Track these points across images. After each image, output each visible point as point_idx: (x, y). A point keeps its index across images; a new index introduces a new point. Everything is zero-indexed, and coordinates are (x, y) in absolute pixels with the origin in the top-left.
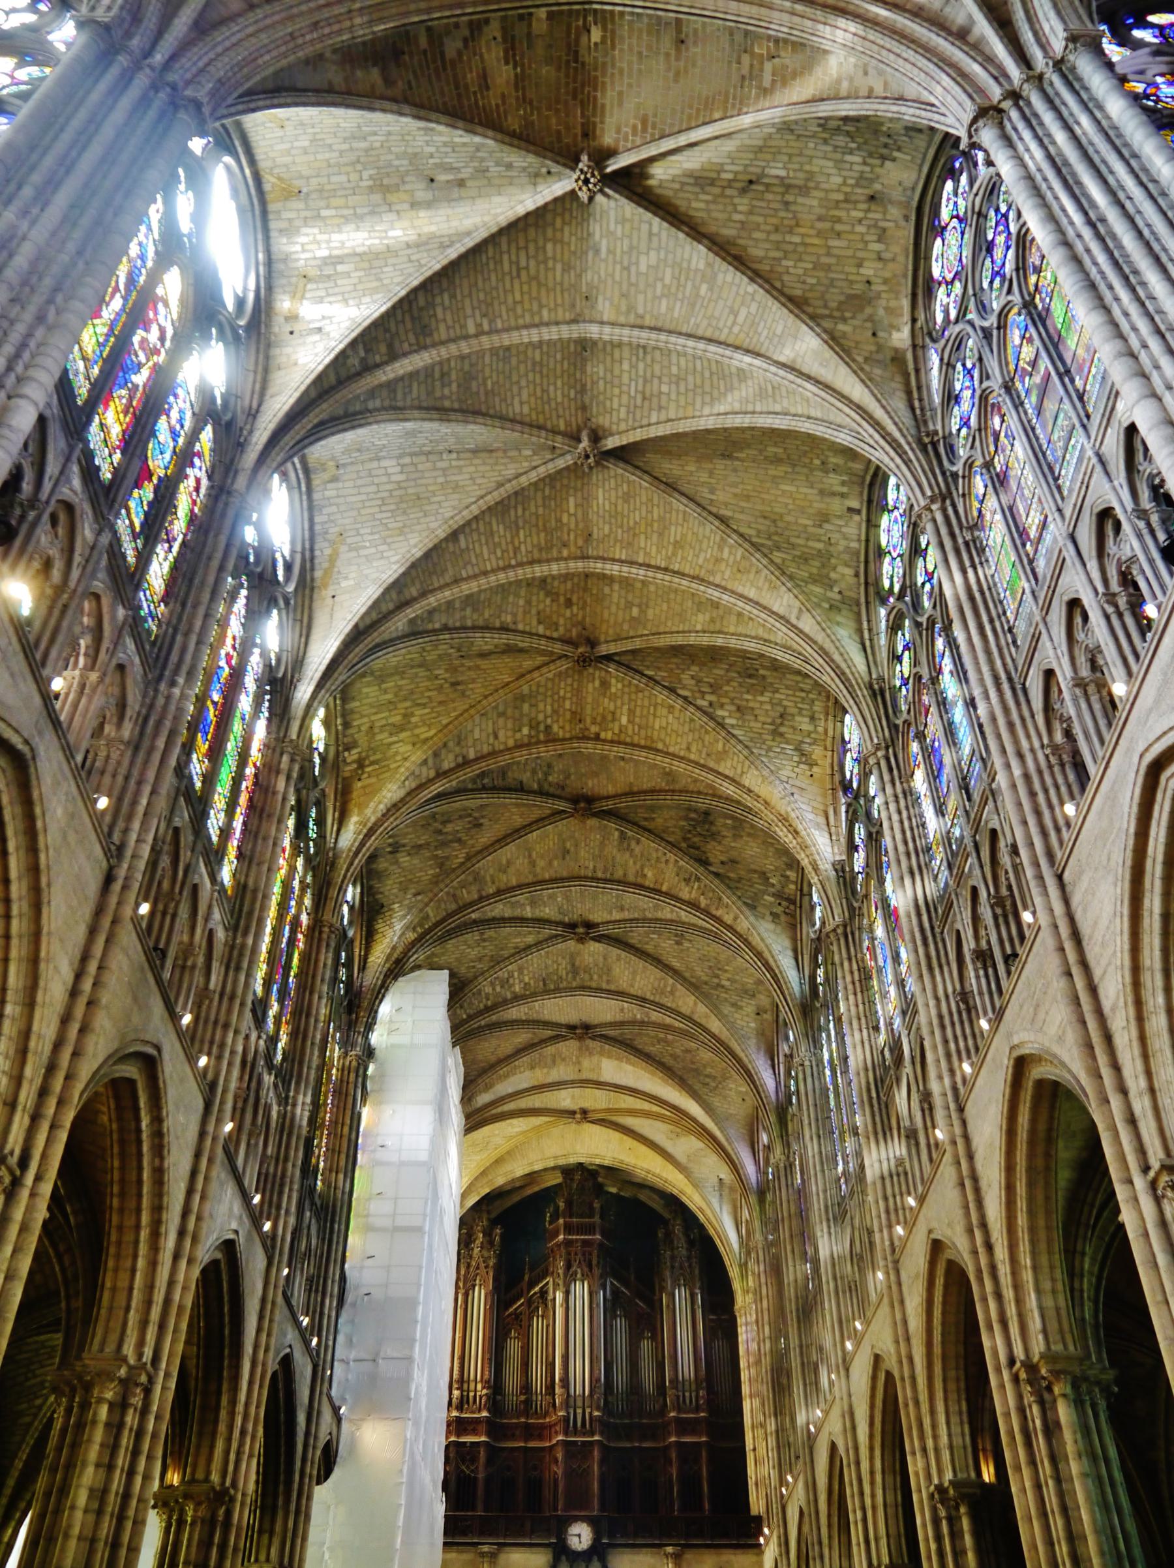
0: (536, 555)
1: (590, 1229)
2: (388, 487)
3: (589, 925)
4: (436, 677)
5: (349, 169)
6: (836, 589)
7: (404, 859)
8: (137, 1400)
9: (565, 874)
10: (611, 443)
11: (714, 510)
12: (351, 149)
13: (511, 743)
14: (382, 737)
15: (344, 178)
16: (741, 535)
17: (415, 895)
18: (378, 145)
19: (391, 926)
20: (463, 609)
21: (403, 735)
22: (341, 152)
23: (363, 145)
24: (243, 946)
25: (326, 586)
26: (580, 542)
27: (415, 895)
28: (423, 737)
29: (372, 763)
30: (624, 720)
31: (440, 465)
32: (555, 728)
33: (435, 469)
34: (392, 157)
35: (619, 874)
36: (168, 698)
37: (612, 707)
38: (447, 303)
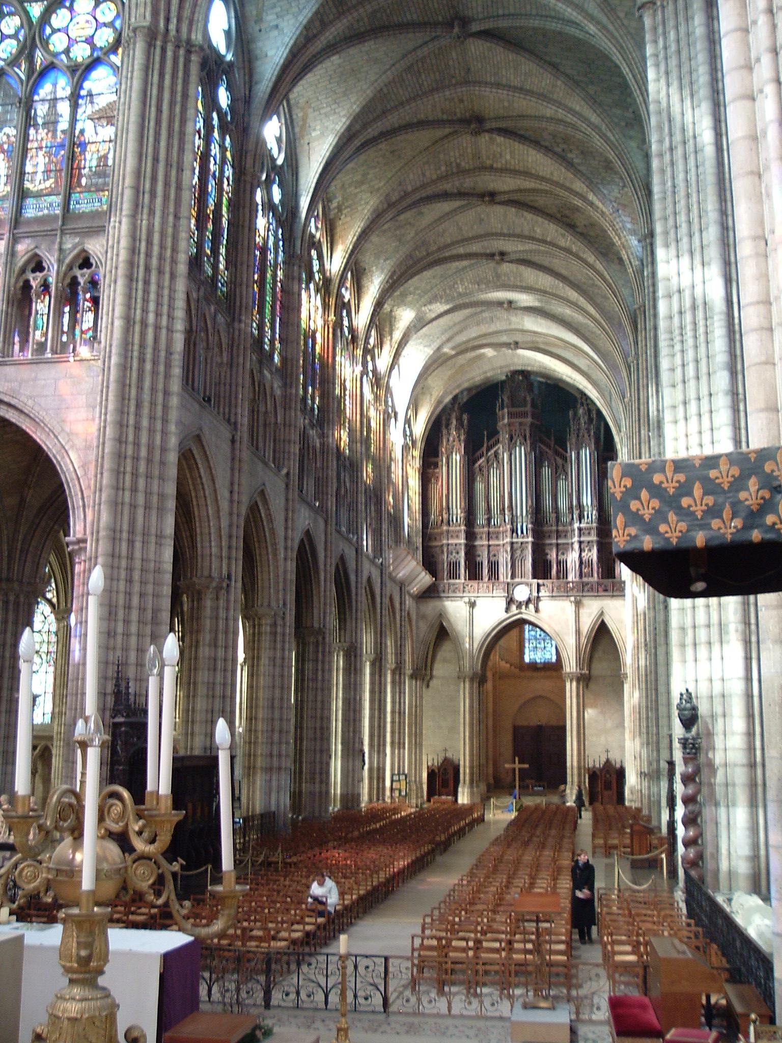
0: (434, 85)
1: (524, 415)
3: (502, 254)
6: (631, 110)
8: (279, 622)
9: (482, 233)
10: (475, 27)
11: (548, 59)
13: (435, 177)
16: (567, 75)
17: (385, 261)
19: (372, 282)
21: (364, 187)
24: (291, 394)
25: (303, 137)
26: (463, 74)
28: (376, 187)
29: (346, 208)
30: (508, 157)
32: (463, 164)
35: (518, 231)
36: (239, 330)
37: (499, 150)
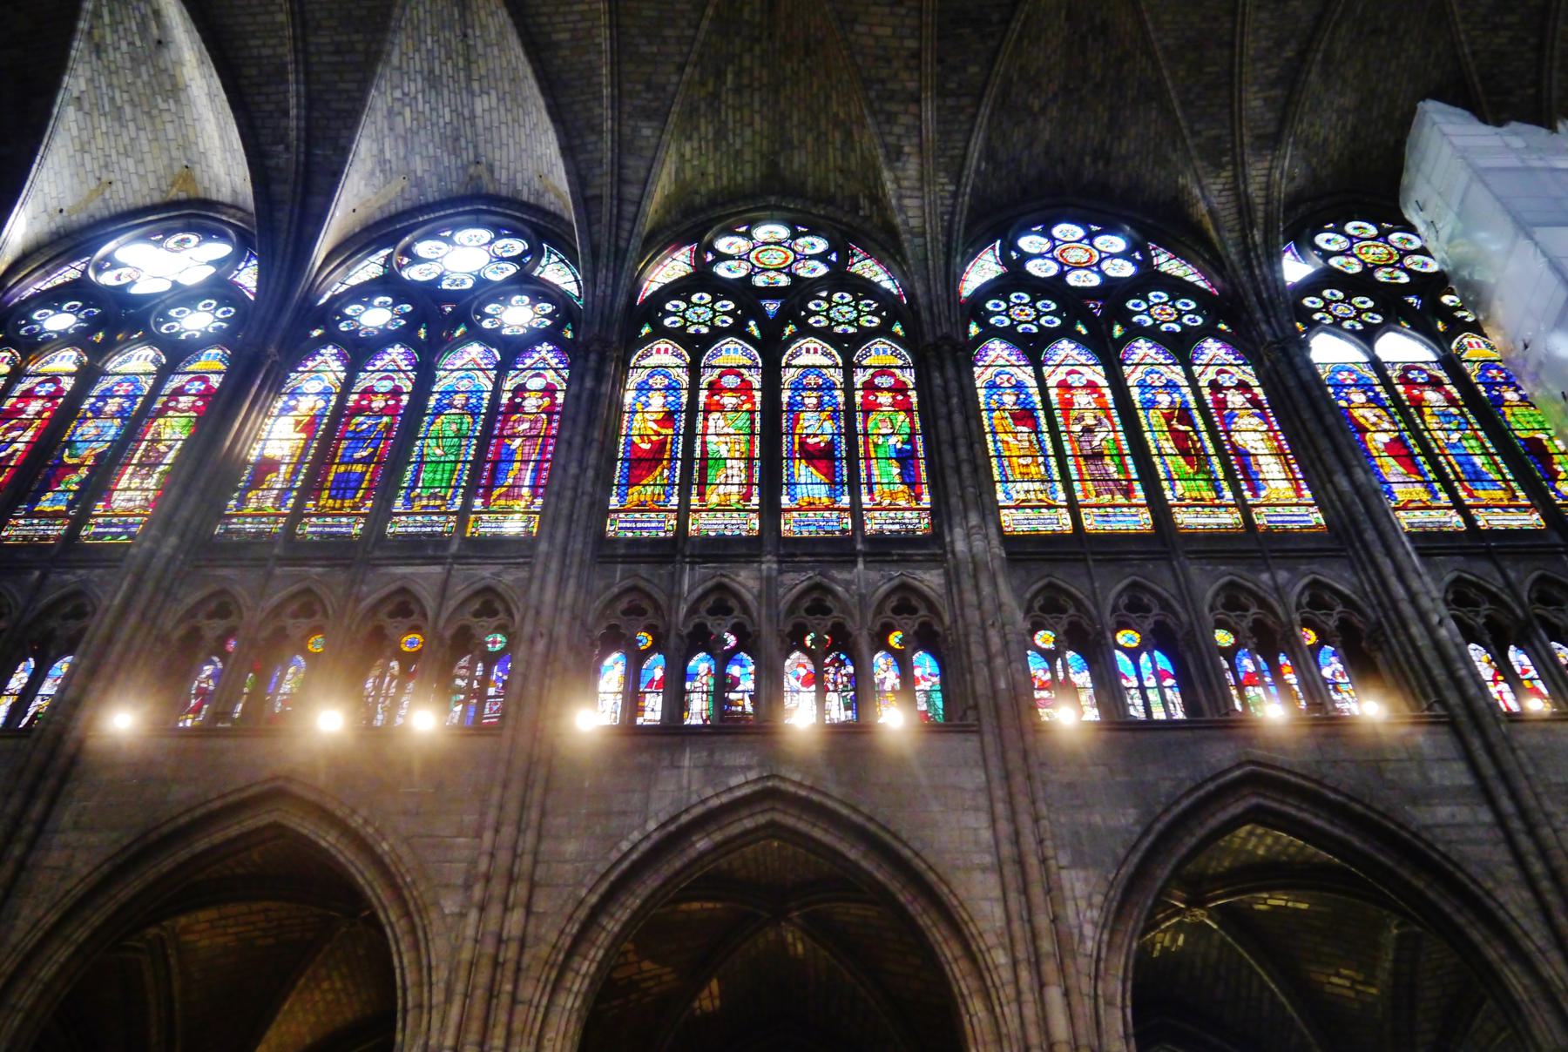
2: (502, 111)
4: (796, 73)
5: (158, 121)
7: (1124, 147)
12: (134, 120)
14: (854, 161)
15: (169, 127)
18: (125, 96)
20: (664, 40)
21: (856, 138)
22: (138, 129)
23: (128, 109)
27: (1175, 150)
31: (480, 50)
33: (485, 55)
34: (139, 84)
38: (259, 42)
